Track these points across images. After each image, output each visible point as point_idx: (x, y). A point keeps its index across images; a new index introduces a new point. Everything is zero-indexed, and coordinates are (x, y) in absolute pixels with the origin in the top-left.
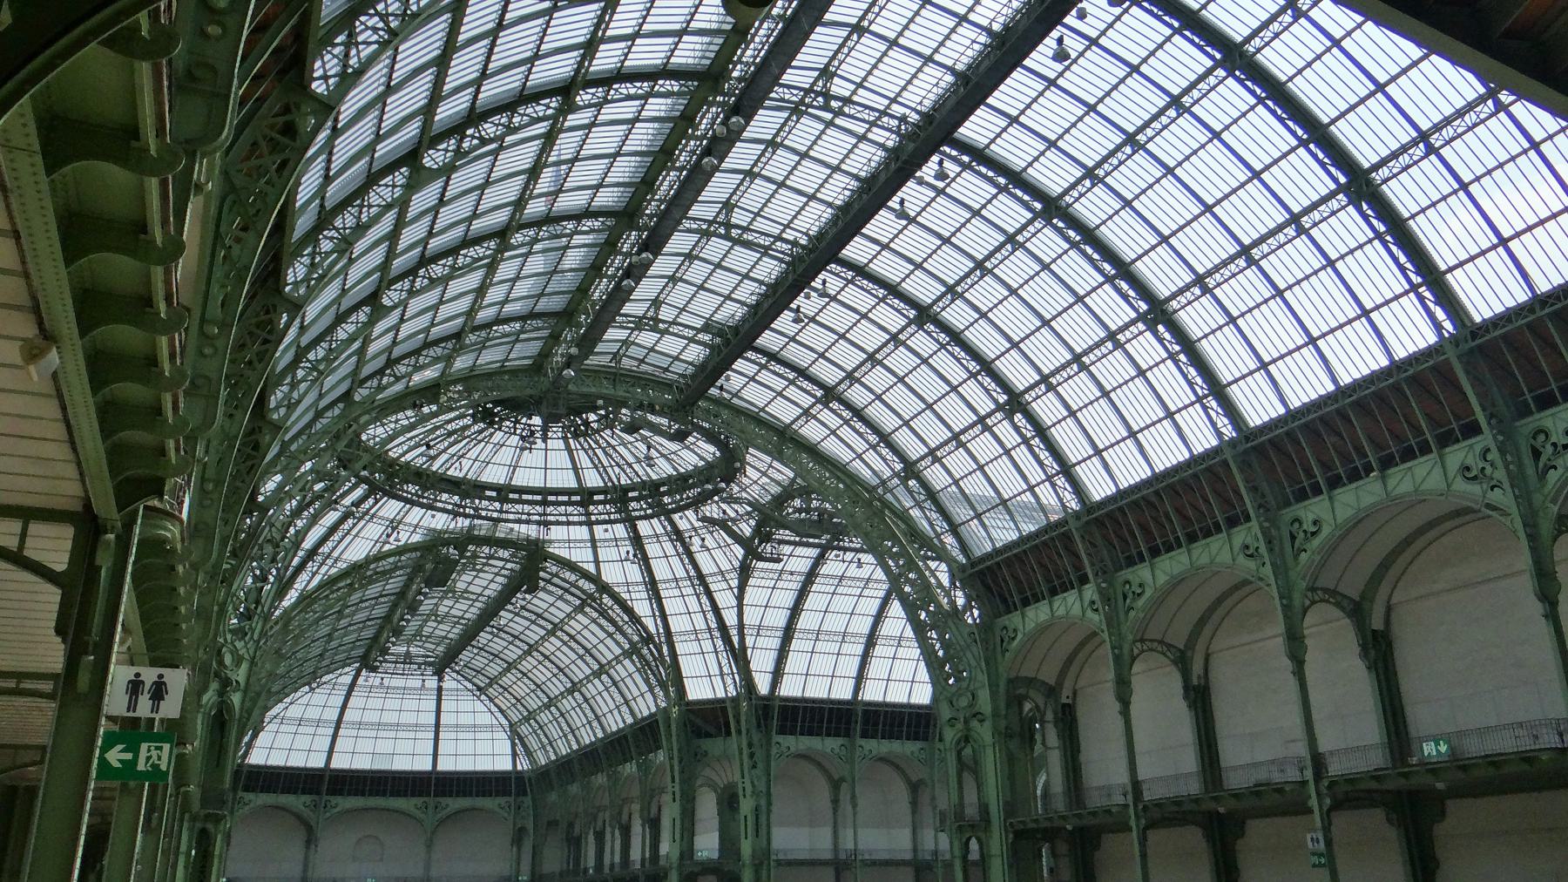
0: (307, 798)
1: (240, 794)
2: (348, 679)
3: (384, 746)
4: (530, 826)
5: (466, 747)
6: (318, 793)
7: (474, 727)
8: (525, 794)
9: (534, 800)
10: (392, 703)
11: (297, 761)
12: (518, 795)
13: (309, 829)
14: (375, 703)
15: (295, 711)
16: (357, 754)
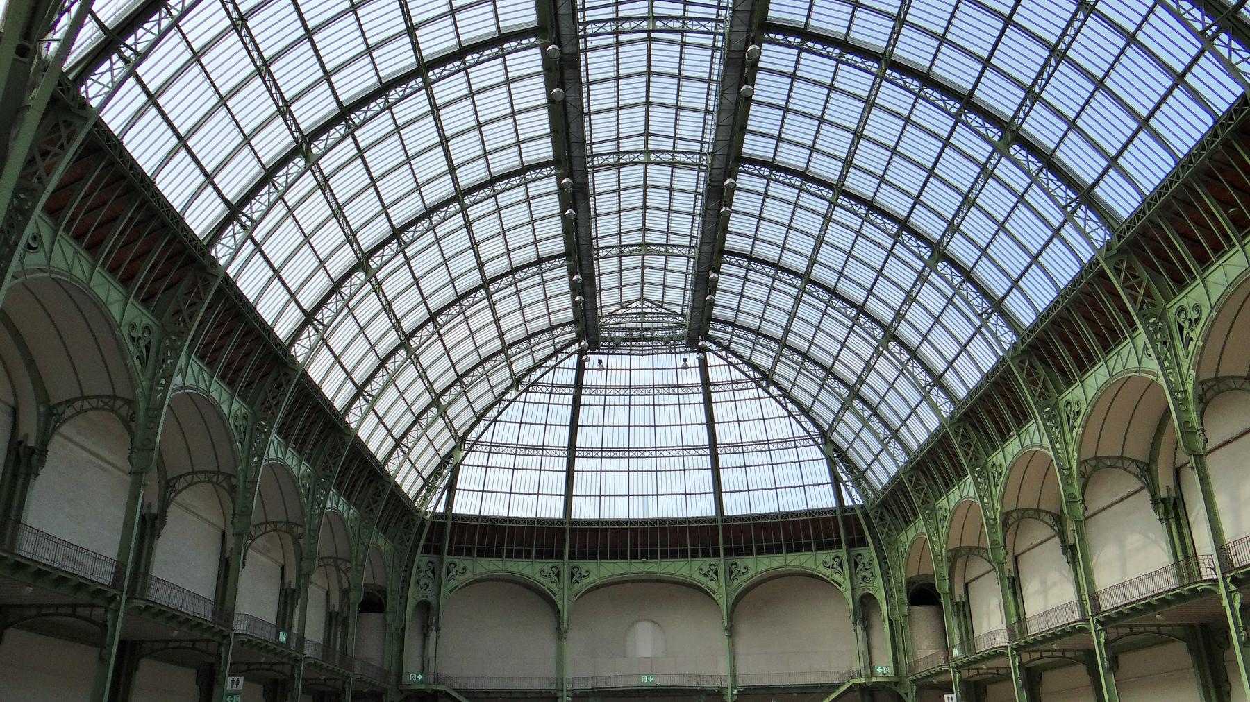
0: (545, 565)
1: (447, 559)
2: (568, 377)
3: (643, 483)
4: (881, 596)
5: (760, 477)
6: (560, 556)
7: (768, 444)
8: (863, 543)
9: (879, 550)
10: (642, 416)
11: (523, 509)
12: (851, 545)
13: (557, 613)
14: (617, 416)
15: (504, 433)
16: (606, 498)
